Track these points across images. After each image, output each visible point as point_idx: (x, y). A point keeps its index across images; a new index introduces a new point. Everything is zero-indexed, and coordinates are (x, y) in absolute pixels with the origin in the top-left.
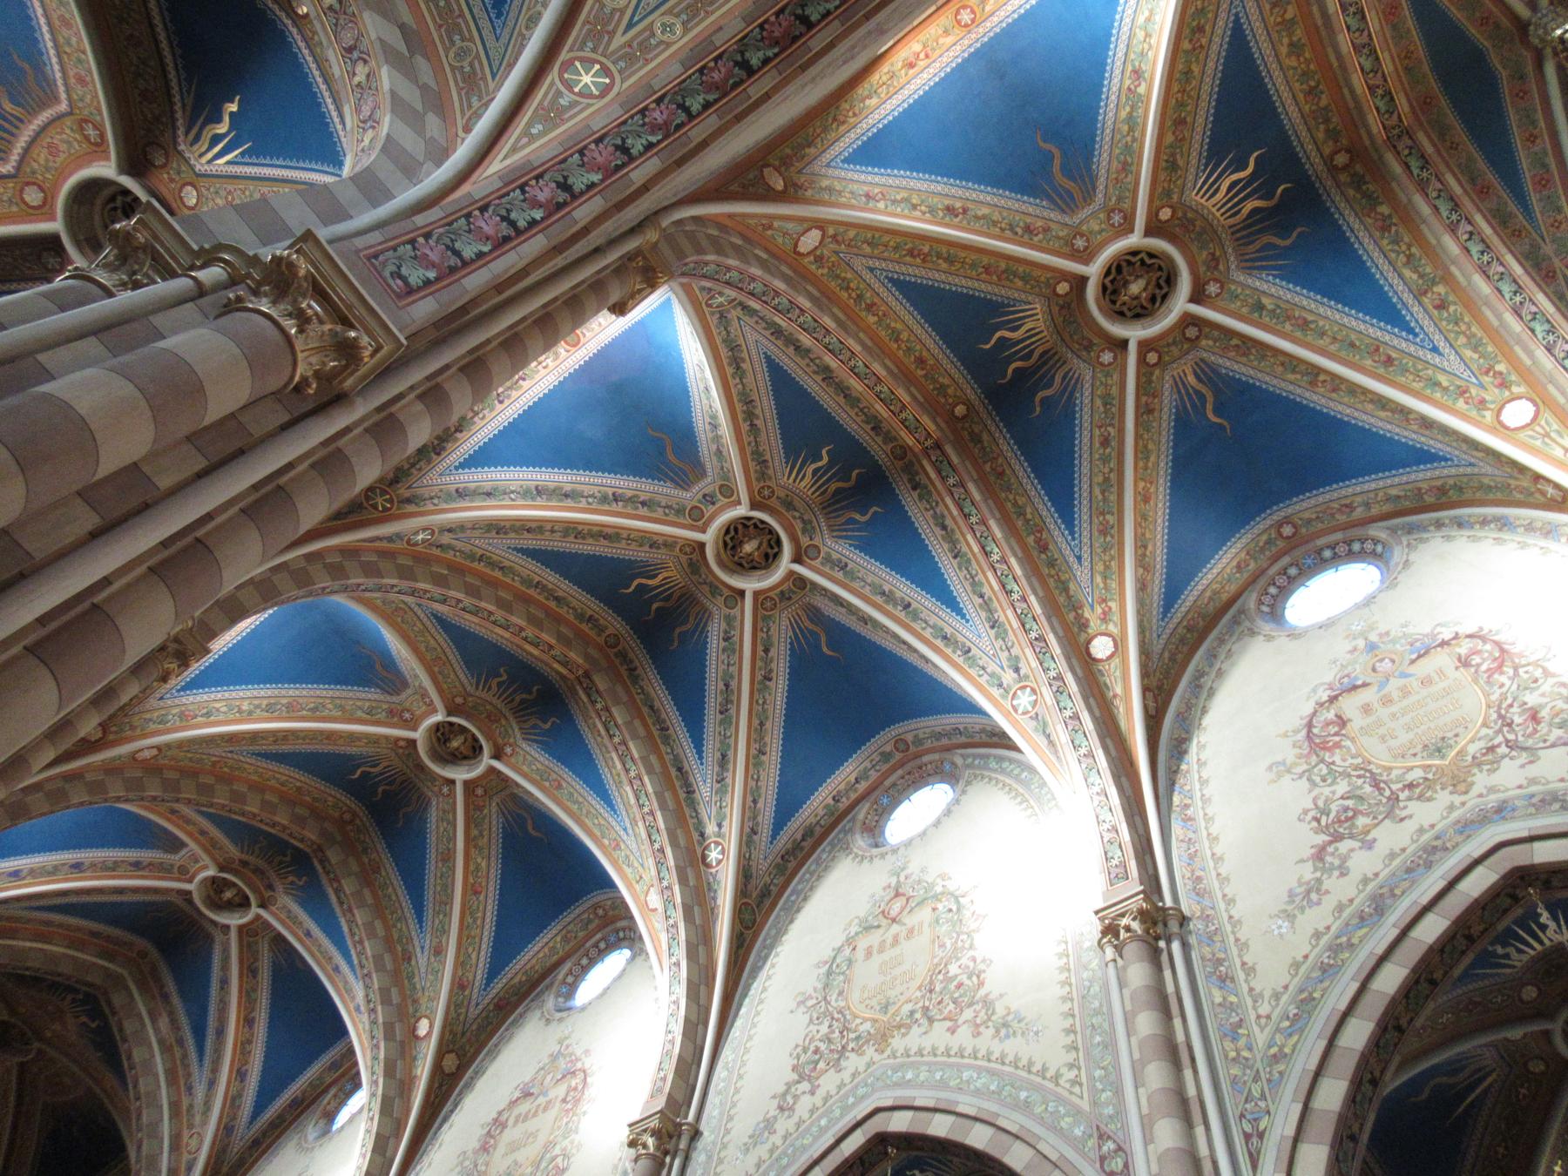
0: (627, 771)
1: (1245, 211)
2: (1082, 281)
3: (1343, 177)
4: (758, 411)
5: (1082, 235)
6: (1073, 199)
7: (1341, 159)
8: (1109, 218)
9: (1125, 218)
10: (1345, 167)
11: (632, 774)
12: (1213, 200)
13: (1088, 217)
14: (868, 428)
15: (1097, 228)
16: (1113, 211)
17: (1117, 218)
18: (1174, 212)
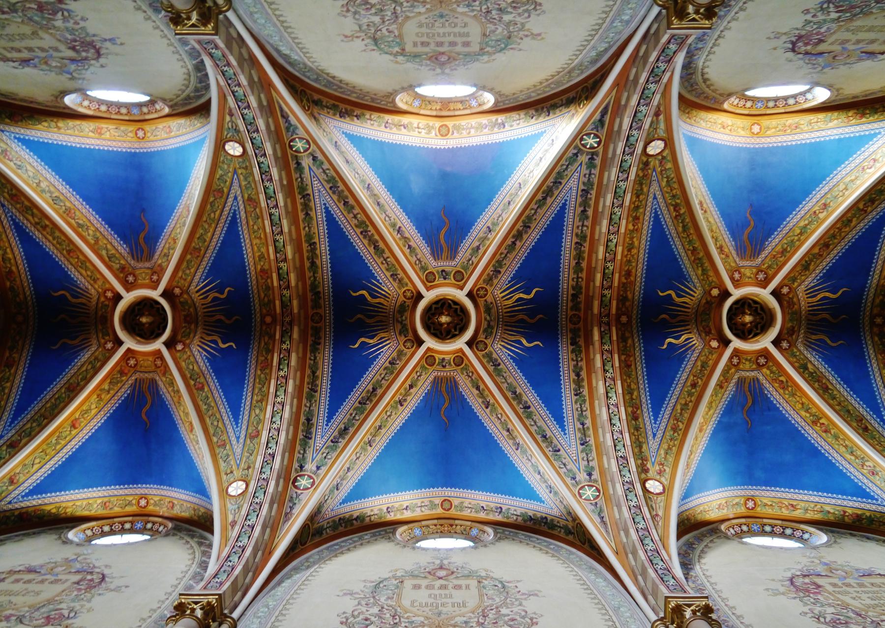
0: (276, 396)
1: (820, 317)
2: (726, 294)
3: (875, 329)
4: (525, 237)
5: (740, 273)
6: (745, 252)
7: (879, 320)
8: (757, 274)
9: (765, 278)
10: (878, 325)
11: (279, 400)
12: (810, 300)
13: (748, 267)
14: (571, 292)
15: (748, 274)
16: (762, 271)
17: (761, 276)
18: (788, 293)
